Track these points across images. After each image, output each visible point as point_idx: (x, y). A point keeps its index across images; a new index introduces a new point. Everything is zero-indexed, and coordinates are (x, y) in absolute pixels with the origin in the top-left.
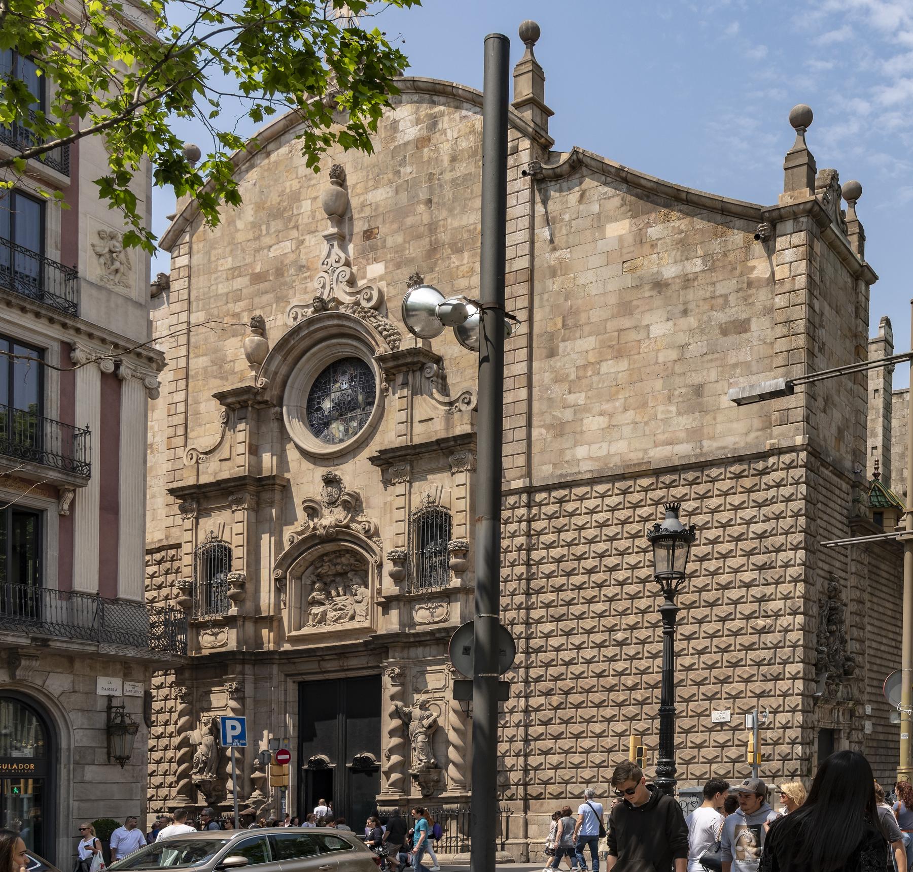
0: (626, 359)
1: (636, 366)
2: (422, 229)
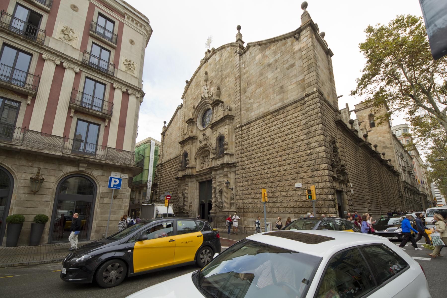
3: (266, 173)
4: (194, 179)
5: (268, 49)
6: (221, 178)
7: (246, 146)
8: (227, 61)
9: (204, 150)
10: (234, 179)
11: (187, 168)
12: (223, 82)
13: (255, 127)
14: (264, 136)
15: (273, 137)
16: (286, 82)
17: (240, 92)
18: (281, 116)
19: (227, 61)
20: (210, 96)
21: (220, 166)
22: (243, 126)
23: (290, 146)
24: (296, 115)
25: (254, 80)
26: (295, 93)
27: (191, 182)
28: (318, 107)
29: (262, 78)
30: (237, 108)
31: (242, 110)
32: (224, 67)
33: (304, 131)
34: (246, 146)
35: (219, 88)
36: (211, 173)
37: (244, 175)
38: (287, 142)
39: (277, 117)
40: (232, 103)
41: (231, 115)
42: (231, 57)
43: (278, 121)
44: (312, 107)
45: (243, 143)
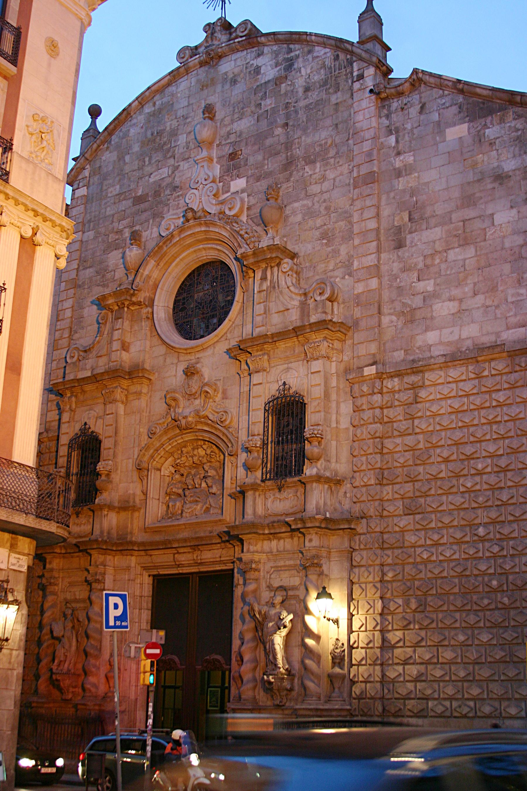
0: (472, 246)
1: (483, 252)
2: (279, 147)
5: (496, 118)
6: (285, 575)
8: (314, 96)
12: (296, 176)
17: (378, 239)
19: (314, 96)
22: (391, 376)
25: (440, 209)
29: (470, 213)
31: (385, 310)
32: (302, 116)
40: (339, 273)
42: (337, 90)
45: (389, 444)
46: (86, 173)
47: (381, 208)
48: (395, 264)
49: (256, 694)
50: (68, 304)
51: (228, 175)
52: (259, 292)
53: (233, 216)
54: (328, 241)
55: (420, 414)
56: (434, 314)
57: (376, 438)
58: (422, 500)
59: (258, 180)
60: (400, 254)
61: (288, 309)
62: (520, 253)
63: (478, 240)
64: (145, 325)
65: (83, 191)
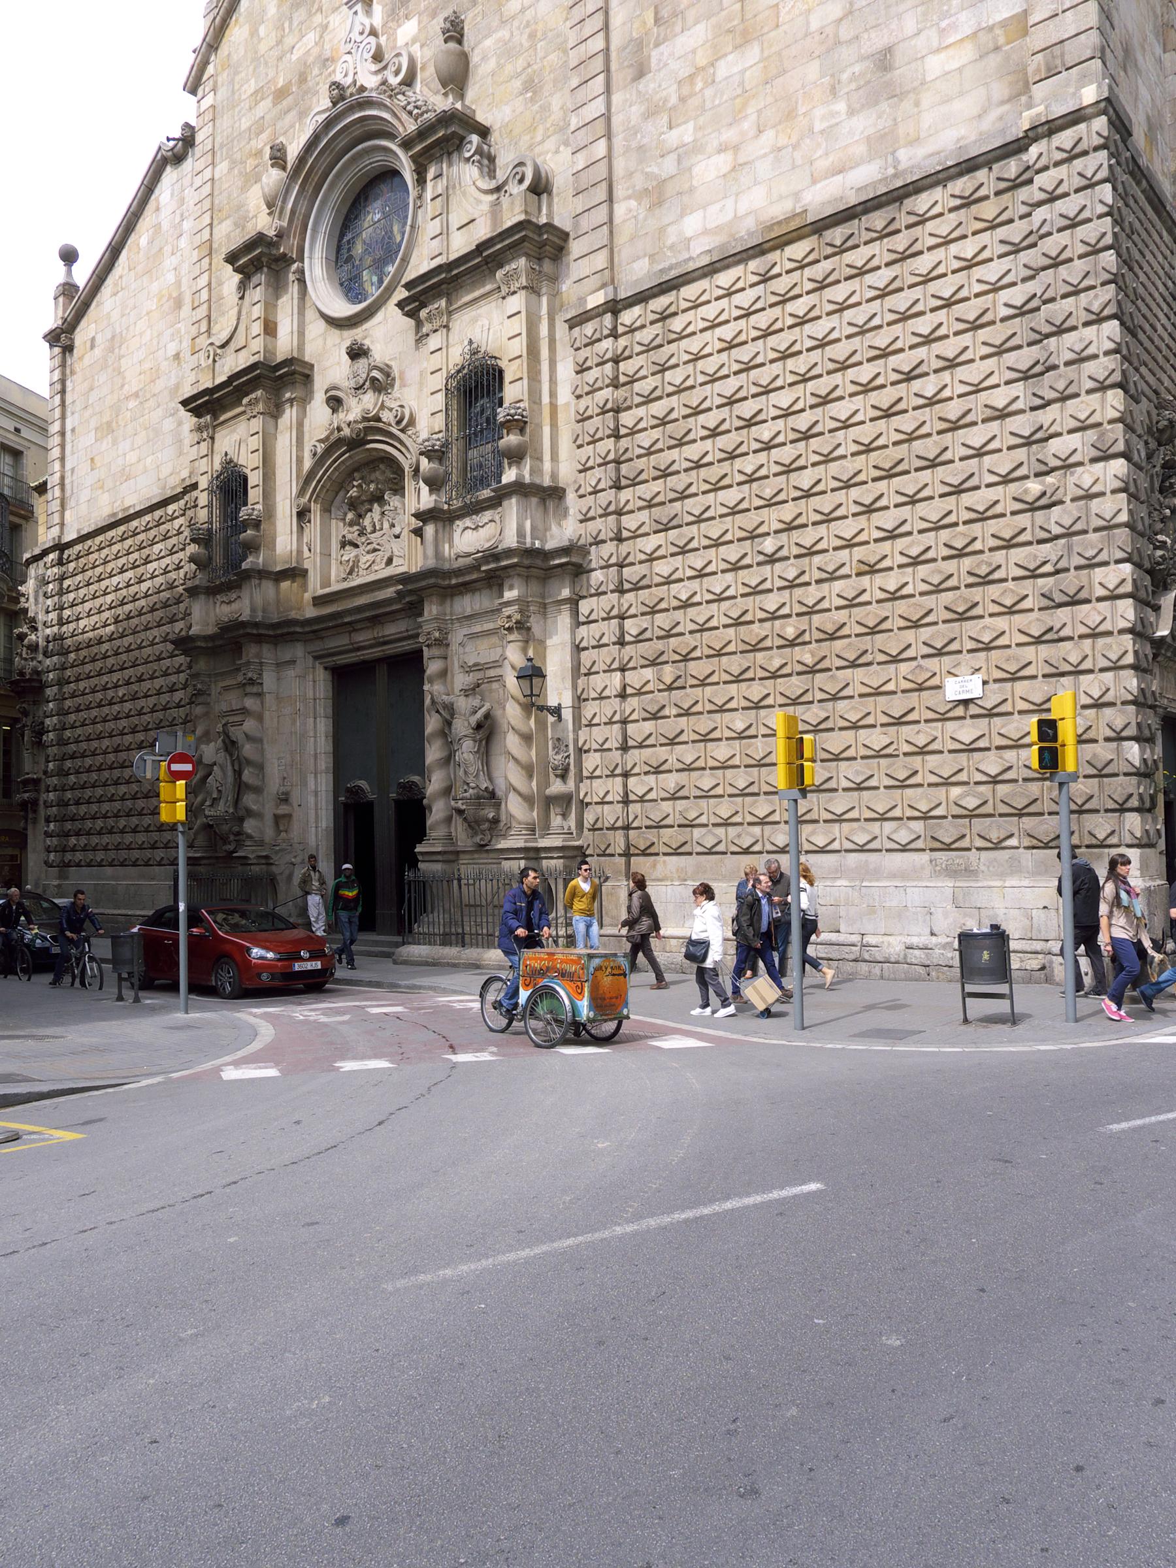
1: (773, 50)
3: (773, 617)
4: (298, 651)
7: (645, 439)
9: (359, 455)
10: (568, 649)
11: (247, 576)
13: (709, 311)
14: (763, 376)
15: (822, 386)
16: (910, 24)
18: (875, 248)
20: (394, 81)
21: (475, 567)
23: (928, 448)
24: (968, 249)
26: (966, 106)
27: (280, 665)
28: (1101, 209)
30: (586, 179)
31: (620, 191)
33: (1010, 358)
34: (645, 439)
35: (455, 32)
36: (414, 608)
37: (632, 627)
38: (907, 423)
39: (849, 257)
40: (550, 144)
41: (549, 226)
43: (854, 284)
44: (1068, 206)
45: (627, 419)
46: (210, 69)
47: (611, 13)
48: (634, 108)
49: (453, 830)
50: (203, 281)
51: (393, 20)
52: (432, 200)
53: (400, 84)
54: (535, 93)
55: (673, 361)
56: (695, 183)
57: (608, 411)
58: (678, 504)
59: (434, 15)
60: (641, 87)
61: (473, 220)
62: (836, 35)
63: (766, 30)
64: (294, 289)
65: (208, 101)
